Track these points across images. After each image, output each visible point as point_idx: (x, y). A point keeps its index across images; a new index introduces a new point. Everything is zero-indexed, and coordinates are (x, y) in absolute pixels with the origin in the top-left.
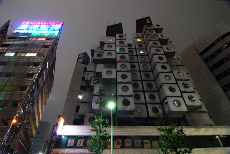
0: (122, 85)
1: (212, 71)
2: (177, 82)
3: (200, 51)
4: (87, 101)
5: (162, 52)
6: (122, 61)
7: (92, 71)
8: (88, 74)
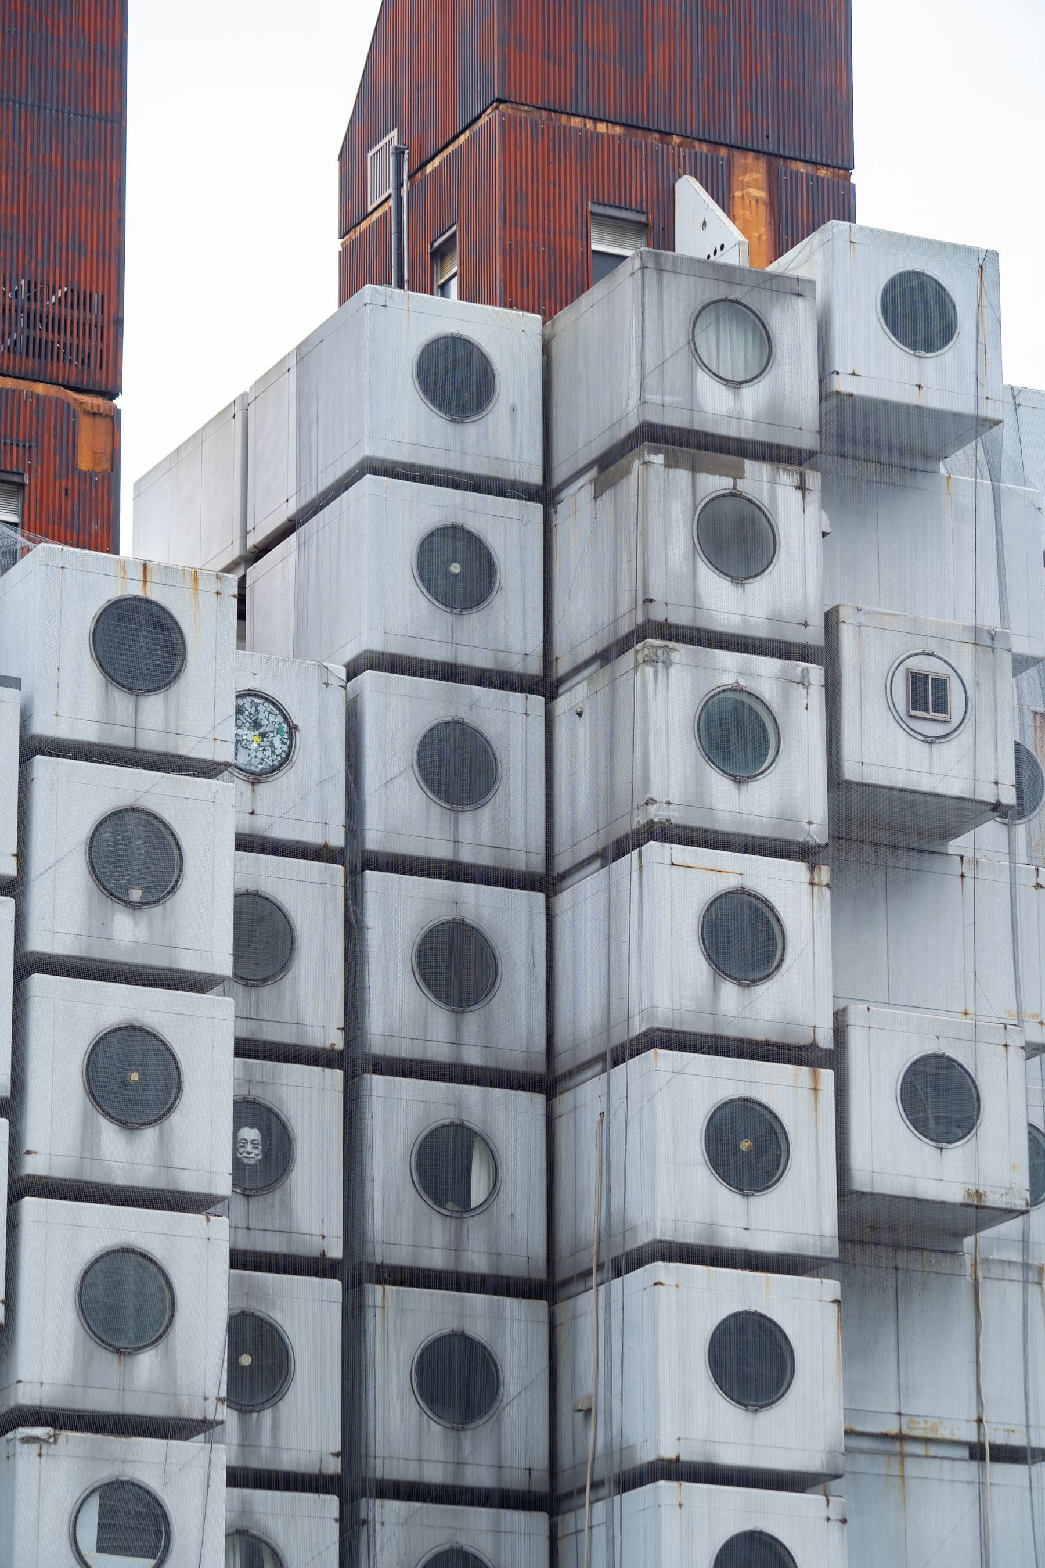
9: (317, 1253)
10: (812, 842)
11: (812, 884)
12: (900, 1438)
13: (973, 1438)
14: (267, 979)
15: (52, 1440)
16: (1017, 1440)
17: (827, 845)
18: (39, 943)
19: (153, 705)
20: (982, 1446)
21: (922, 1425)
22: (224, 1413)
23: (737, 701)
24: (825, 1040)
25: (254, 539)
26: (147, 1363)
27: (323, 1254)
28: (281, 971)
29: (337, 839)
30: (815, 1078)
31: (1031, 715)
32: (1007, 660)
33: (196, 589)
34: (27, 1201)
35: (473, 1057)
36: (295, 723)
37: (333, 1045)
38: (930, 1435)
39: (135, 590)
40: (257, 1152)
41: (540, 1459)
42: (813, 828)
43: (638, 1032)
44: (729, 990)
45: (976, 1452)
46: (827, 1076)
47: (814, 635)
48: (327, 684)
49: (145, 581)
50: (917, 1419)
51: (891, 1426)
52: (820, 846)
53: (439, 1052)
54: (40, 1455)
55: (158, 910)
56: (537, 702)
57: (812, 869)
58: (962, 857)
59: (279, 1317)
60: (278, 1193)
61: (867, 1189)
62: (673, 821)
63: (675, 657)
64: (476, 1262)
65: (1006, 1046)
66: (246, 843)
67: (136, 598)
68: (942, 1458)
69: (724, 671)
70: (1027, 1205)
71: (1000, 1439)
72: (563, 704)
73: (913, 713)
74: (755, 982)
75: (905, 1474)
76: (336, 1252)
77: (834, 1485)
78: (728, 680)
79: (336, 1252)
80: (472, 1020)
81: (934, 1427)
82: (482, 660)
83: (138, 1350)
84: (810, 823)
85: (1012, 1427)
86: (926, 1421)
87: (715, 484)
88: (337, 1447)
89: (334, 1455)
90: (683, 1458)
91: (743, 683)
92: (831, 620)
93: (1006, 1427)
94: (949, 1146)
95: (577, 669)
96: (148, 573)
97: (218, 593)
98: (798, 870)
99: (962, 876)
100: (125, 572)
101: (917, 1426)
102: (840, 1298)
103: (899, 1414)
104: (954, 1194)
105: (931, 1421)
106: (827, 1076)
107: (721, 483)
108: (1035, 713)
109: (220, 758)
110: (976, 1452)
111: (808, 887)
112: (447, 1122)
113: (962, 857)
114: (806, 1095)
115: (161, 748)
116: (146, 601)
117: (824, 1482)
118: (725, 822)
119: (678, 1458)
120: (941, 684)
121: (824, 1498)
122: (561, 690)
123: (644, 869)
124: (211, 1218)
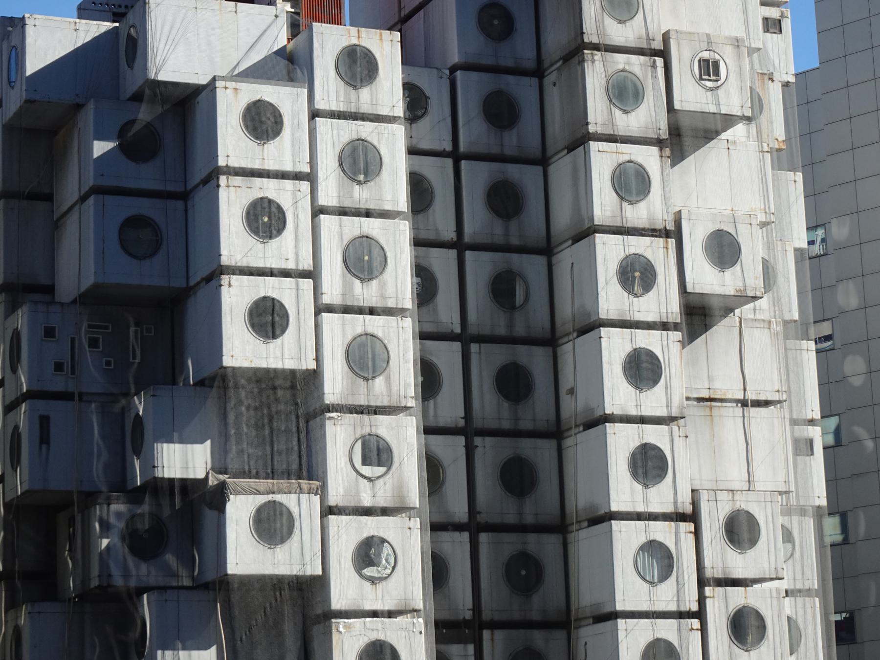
2: (702, 600)
6: (362, 401)
9: (450, 331)
10: (661, 138)
11: (662, 157)
12: (711, 400)
13: (741, 397)
14: (422, 211)
15: (340, 418)
16: (762, 397)
17: (667, 139)
18: (322, 201)
19: (365, 93)
20: (747, 400)
21: (719, 393)
22: (411, 403)
23: (625, 76)
24: (671, 227)
25: (403, 14)
26: (379, 383)
27: (453, 331)
28: (427, 207)
29: (448, 147)
30: (667, 242)
31: (756, 74)
32: (746, 50)
33: (381, 39)
34: (324, 315)
35: (515, 241)
36: (428, 95)
37: (452, 238)
38: (723, 397)
39: (354, 41)
40: (420, 288)
41: (552, 416)
42: (661, 131)
43: (587, 227)
44: (625, 205)
45: (744, 403)
46: (672, 242)
47: (658, 45)
48: (441, 77)
49: (359, 37)
50: (717, 390)
51: (705, 394)
52: (664, 139)
53: (499, 240)
54: (335, 425)
55: (372, 183)
56: (534, 81)
57: (661, 150)
58: (728, 140)
59: (434, 360)
60: (431, 305)
61: (692, 291)
62: (599, 132)
63: (596, 58)
64: (520, 330)
65: (751, 224)
67: (355, 45)
68: (729, 407)
69: (618, 63)
70: (763, 294)
71: (754, 397)
72: (548, 81)
73: (704, 77)
74: (638, 202)
75: (713, 415)
76: (458, 330)
77: (682, 422)
78: (621, 67)
79: (458, 330)
80: (513, 224)
81: (725, 394)
82: (510, 63)
83: (374, 378)
84: (659, 129)
85: (759, 392)
86: (721, 391)
88: (463, 415)
89: (461, 418)
90: (615, 413)
91: (627, 68)
92: (666, 37)
93: (757, 392)
94: (727, 270)
95: (552, 65)
96: (360, 33)
97: (391, 41)
98: (655, 150)
99: (728, 149)
100: (350, 34)
101: (717, 393)
102: (681, 340)
103: (709, 389)
104: (731, 291)
105: (723, 391)
106: (672, 242)
108: (758, 73)
109: (396, 115)
110: (744, 403)
111: (658, 158)
112: (504, 270)
113: (728, 140)
114: (661, 251)
115: (370, 112)
116: (359, 46)
117: (677, 420)
118: (621, 131)
119: (613, 413)
120: (716, 64)
121: (678, 427)
122: (546, 74)
123: (586, 154)
124: (403, 318)
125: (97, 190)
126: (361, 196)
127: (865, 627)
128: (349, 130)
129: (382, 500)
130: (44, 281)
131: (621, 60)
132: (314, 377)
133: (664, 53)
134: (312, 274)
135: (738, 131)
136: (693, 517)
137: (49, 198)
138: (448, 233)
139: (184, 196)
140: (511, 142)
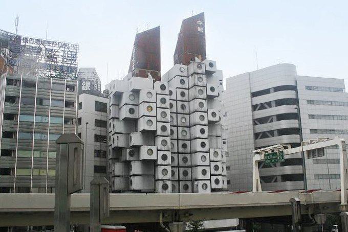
0: (163, 167)
1: (255, 124)
3: (254, 90)
4: (121, 175)
5: (206, 122)
7: (122, 133)
8: (118, 136)
66: (170, 100)
87: (199, 76)
107: (199, 76)
125: (126, 104)
126: (163, 106)
127: (231, 168)
128: (162, 96)
129: (166, 149)
130: (117, 117)
131: (200, 88)
132: (156, 131)
133: (206, 87)
134: (156, 117)
135: (216, 98)
136: (209, 152)
137: (119, 105)
138: (175, 112)
139: (138, 105)
140: (184, 99)
